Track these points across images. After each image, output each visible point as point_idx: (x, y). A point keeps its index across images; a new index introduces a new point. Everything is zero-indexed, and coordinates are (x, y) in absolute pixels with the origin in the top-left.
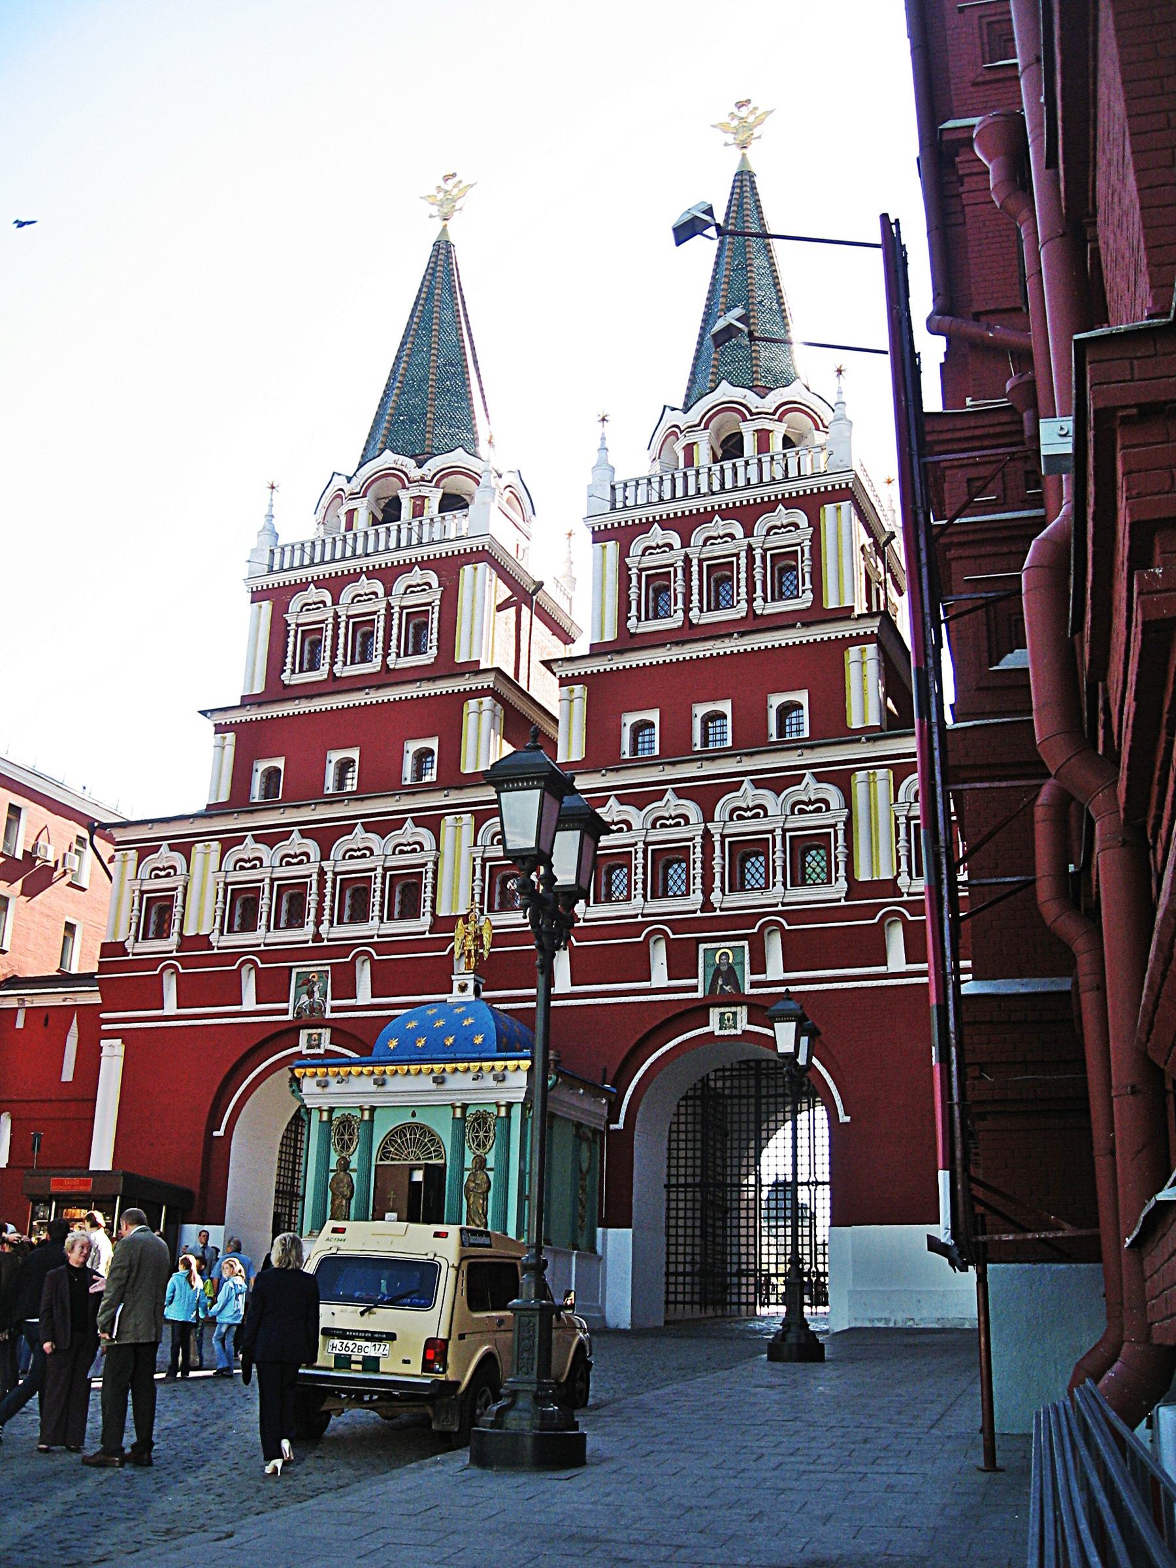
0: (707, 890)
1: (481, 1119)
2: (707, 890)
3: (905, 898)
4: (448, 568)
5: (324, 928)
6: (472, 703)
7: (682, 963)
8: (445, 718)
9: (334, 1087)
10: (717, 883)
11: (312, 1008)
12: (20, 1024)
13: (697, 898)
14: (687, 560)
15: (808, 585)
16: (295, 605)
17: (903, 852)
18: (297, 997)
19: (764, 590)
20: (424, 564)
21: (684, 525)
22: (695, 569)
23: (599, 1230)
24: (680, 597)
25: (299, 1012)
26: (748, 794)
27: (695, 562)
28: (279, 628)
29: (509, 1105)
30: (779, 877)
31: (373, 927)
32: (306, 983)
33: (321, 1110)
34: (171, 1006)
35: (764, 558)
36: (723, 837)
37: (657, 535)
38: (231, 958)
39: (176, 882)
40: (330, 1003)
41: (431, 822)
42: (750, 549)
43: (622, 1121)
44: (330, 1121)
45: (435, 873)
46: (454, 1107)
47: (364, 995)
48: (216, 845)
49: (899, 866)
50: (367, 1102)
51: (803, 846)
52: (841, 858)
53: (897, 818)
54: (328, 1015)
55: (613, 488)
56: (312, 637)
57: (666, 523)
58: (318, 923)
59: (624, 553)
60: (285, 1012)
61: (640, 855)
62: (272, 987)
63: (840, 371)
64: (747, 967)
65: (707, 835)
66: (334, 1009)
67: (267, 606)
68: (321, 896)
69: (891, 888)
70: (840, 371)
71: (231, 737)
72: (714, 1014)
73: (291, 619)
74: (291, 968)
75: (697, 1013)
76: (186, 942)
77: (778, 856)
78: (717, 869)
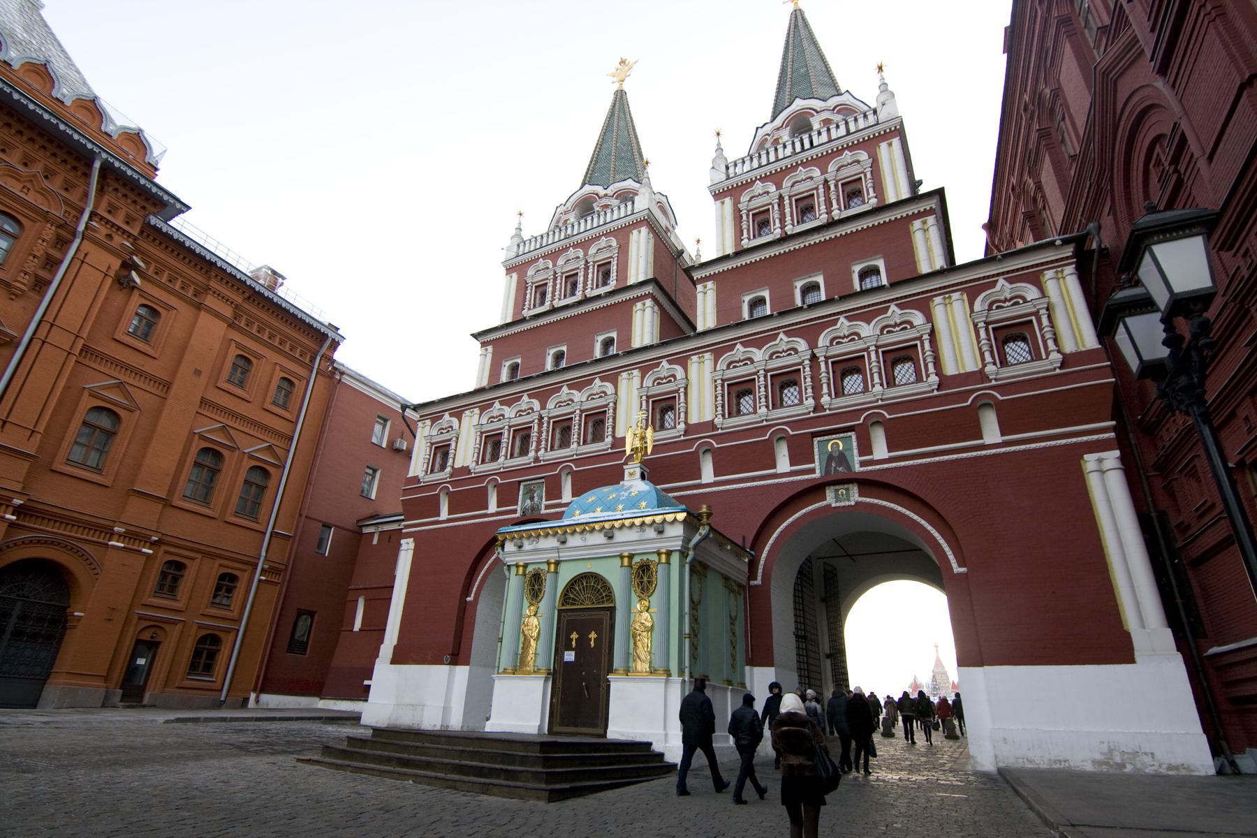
0: (817, 396)
1: (645, 568)
2: (817, 396)
3: (994, 383)
4: (622, 234)
6: (639, 305)
7: (801, 453)
8: (621, 315)
9: (527, 546)
10: (825, 390)
11: (533, 509)
12: (375, 542)
13: (810, 402)
14: (781, 198)
15: (872, 194)
17: (985, 348)
18: (524, 501)
19: (838, 203)
20: (607, 235)
21: (776, 178)
22: (787, 202)
23: (747, 668)
24: (777, 221)
26: (843, 325)
27: (786, 198)
28: (522, 287)
29: (669, 553)
30: (876, 379)
31: (574, 449)
33: (517, 566)
34: (444, 514)
35: (836, 186)
36: (827, 358)
37: (759, 187)
38: (481, 478)
39: (452, 435)
40: (544, 503)
41: (613, 378)
42: (826, 181)
43: (759, 578)
44: (524, 575)
45: (615, 409)
46: (622, 557)
48: (477, 411)
49: (983, 359)
50: (553, 557)
51: (898, 355)
52: (929, 359)
53: (975, 325)
54: (543, 511)
55: (727, 168)
56: (541, 290)
57: (762, 179)
58: (537, 450)
60: (515, 511)
61: (762, 379)
63: (880, 68)
64: (856, 452)
65: (814, 358)
66: (547, 507)
67: (515, 275)
68: (540, 433)
69: (980, 376)
70: (880, 68)
71: (490, 348)
74: (520, 482)
75: (816, 490)
76: (456, 472)
77: (873, 362)
78: (824, 380)
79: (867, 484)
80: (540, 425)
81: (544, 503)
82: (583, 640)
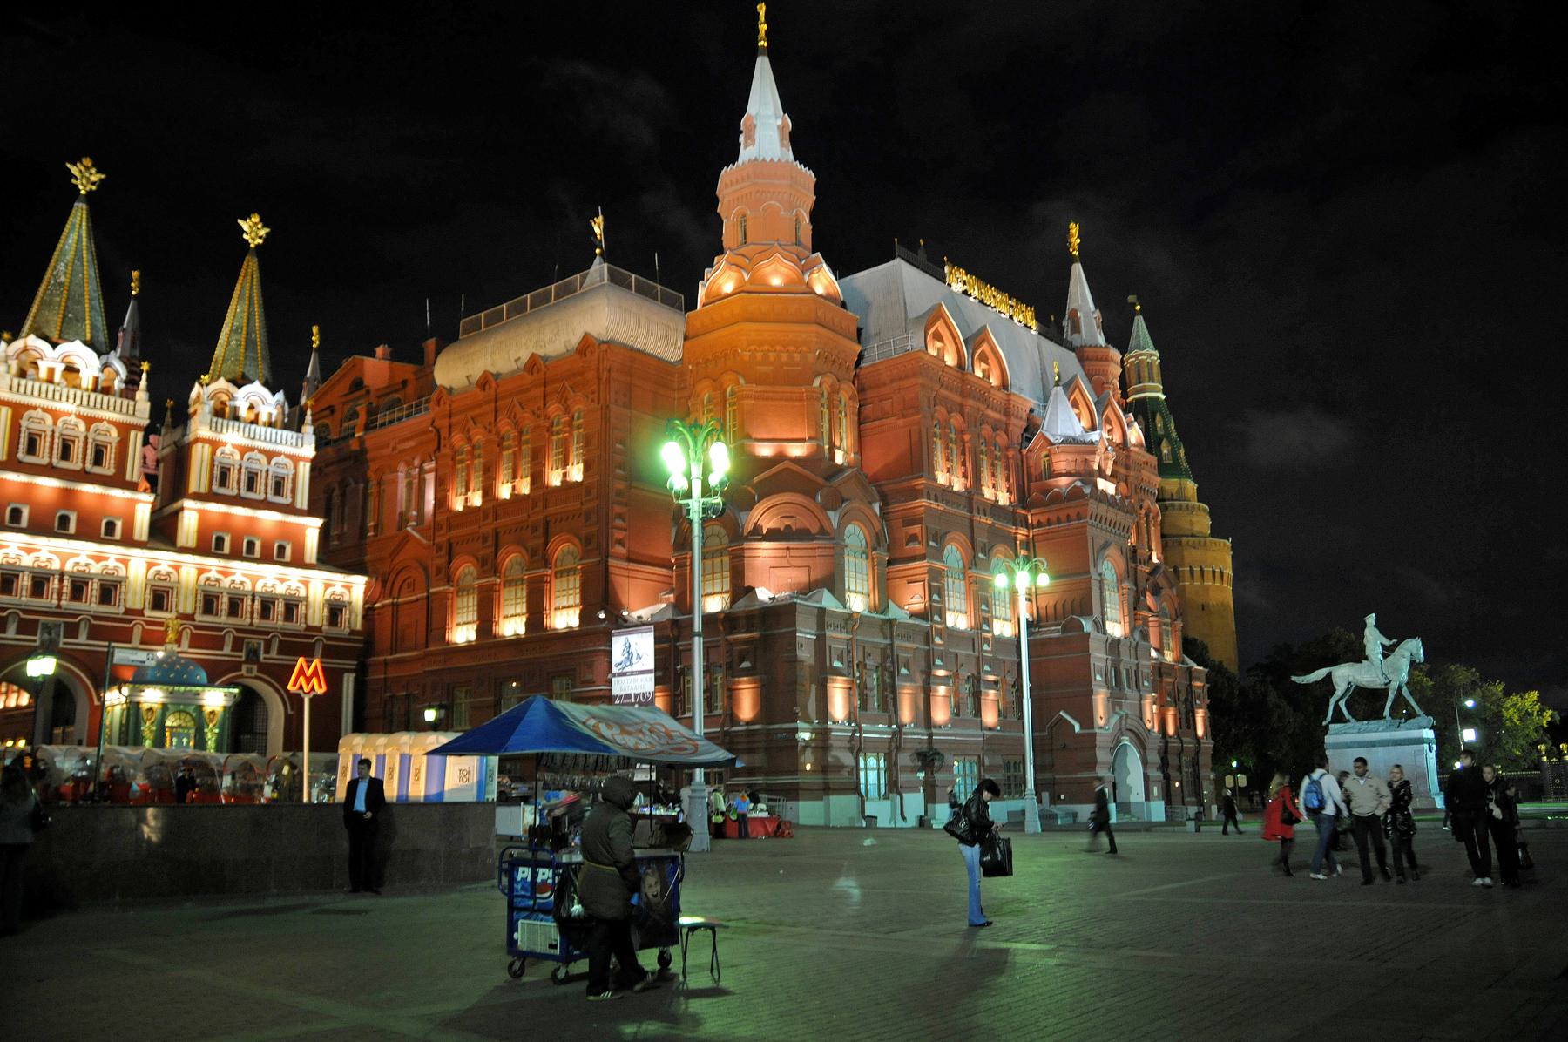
5: (63, 603)
7: (237, 645)
11: (51, 641)
16: (26, 415)
25: (42, 642)
31: (94, 607)
32: (47, 628)
40: (63, 640)
47: (83, 638)
58: (59, 599)
59: (213, 453)
62: (27, 627)
69: (319, 629)
72: (244, 667)
73: (24, 423)
75: (237, 666)
79: (264, 668)
80: (61, 580)
81: (63, 640)
82: (180, 742)
